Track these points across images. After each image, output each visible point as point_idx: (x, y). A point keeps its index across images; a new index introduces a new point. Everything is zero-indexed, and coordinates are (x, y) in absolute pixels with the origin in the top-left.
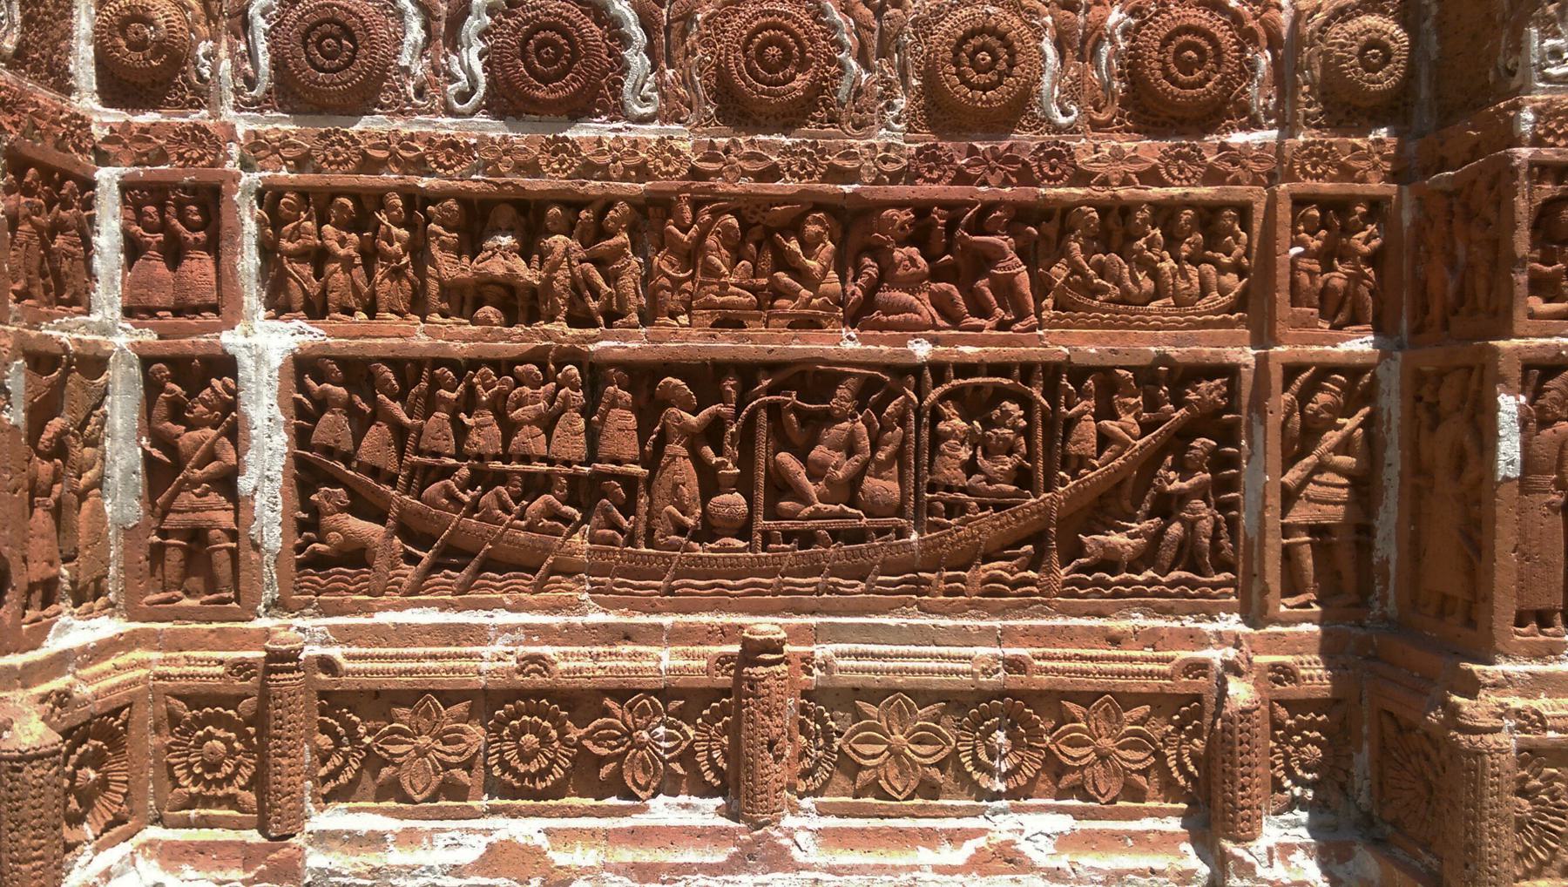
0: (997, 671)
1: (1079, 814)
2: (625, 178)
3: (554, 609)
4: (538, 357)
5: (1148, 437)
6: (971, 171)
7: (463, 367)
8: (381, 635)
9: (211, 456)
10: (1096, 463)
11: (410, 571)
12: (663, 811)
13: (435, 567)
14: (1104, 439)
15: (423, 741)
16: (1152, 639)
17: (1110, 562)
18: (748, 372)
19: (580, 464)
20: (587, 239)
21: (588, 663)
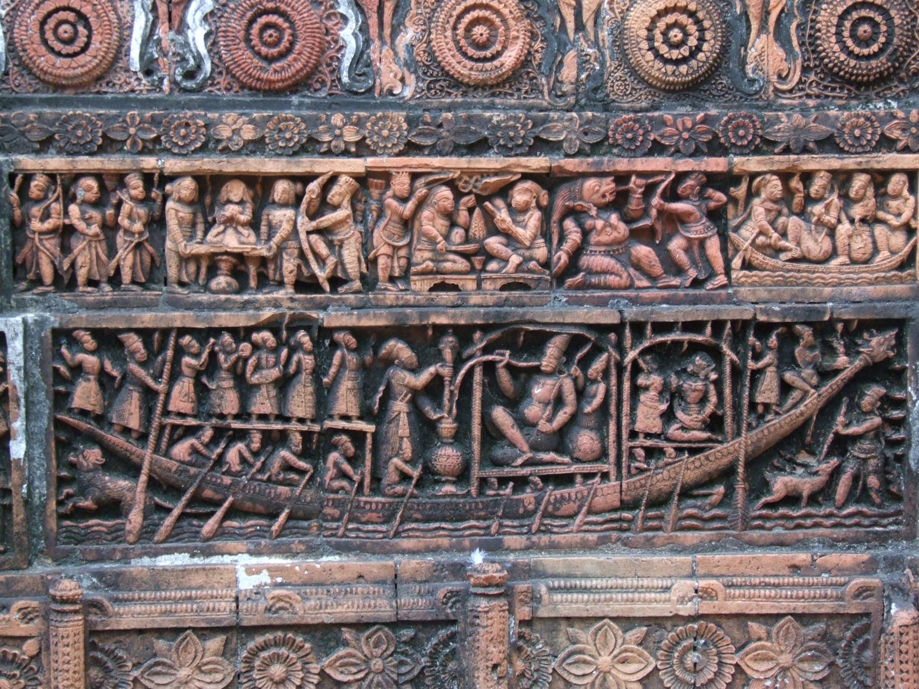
4: (273, 326)
7: (203, 335)
14: (785, 388)
17: (792, 499)
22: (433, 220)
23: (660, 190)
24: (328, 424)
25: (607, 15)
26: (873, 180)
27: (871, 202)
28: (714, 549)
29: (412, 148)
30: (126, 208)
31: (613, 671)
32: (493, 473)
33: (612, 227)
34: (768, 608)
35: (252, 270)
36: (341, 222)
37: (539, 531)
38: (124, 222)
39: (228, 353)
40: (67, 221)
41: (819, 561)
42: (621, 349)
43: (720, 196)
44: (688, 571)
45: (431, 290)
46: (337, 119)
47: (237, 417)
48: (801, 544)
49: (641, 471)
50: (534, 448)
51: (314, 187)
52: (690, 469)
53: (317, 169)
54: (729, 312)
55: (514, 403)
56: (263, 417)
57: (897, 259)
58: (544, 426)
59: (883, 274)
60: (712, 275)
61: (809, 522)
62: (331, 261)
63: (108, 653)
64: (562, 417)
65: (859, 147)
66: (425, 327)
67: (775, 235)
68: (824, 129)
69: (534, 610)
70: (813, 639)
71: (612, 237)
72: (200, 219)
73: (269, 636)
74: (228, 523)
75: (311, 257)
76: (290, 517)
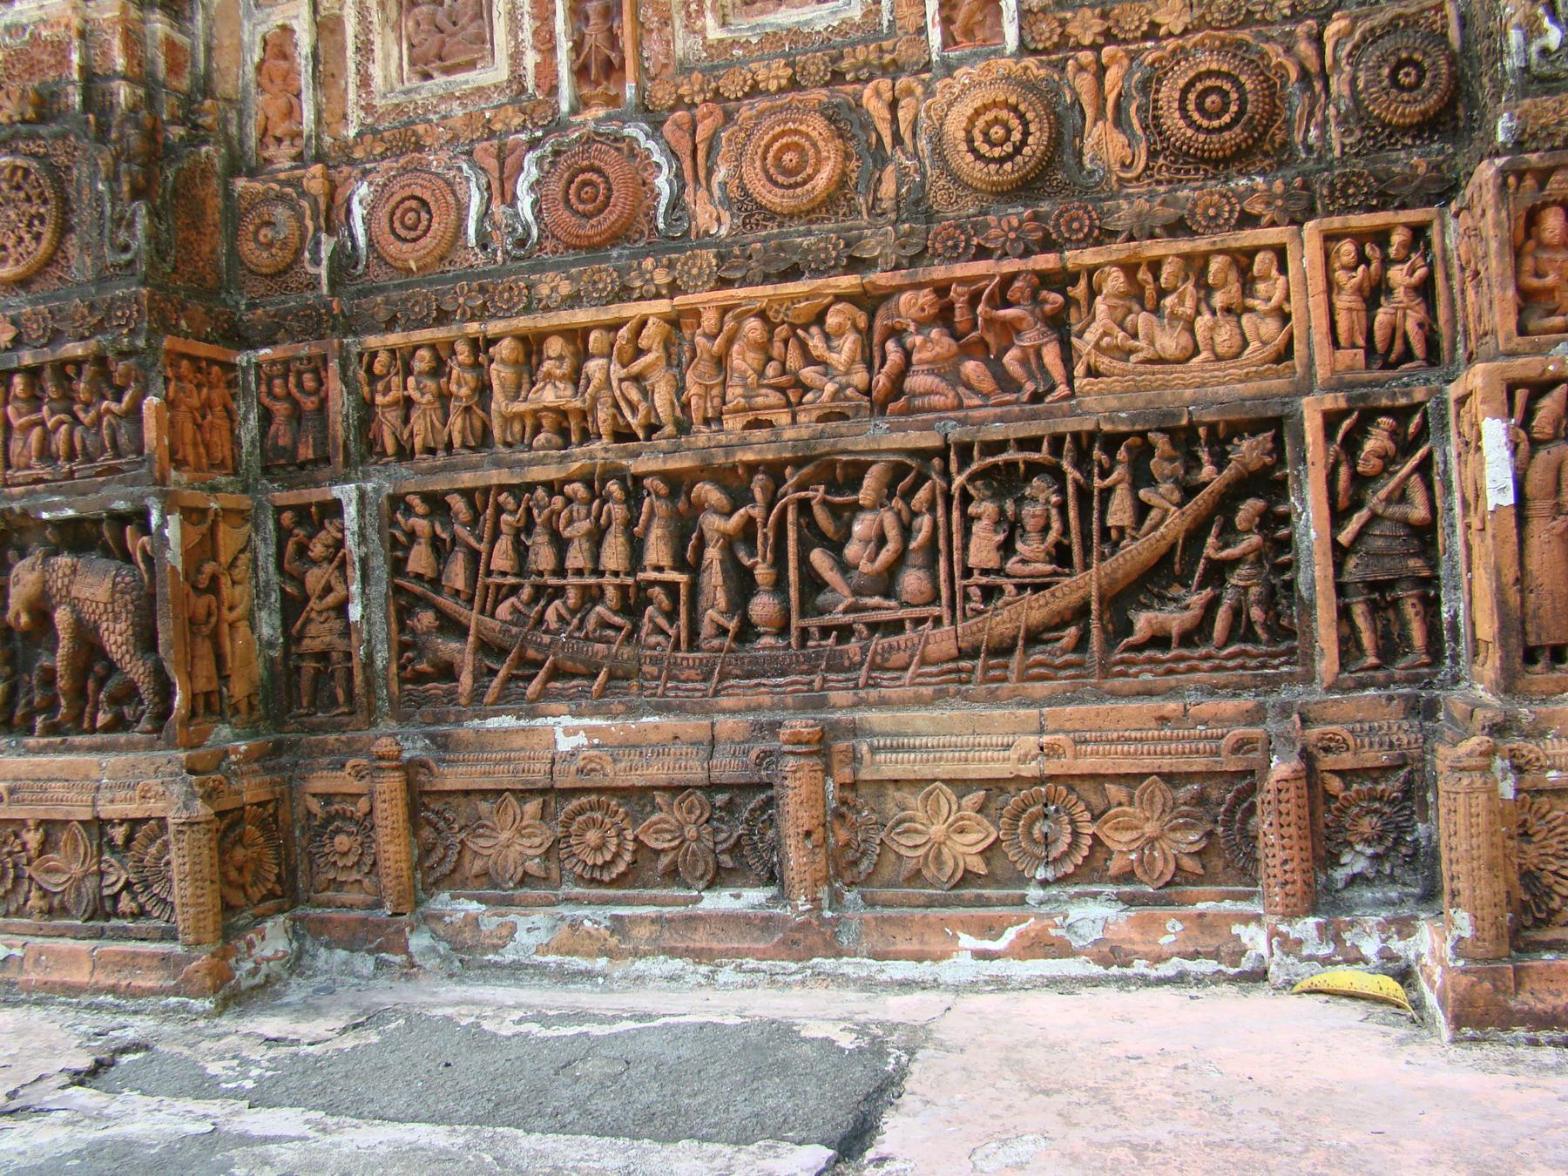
9: (328, 589)
14: (1142, 510)
17: (1159, 641)
20: (626, 358)
24: (641, 576)
25: (924, 123)
26: (1235, 262)
27: (1235, 287)
28: (1070, 701)
29: (724, 283)
32: (813, 623)
33: (936, 343)
34: (1127, 766)
35: (573, 424)
37: (867, 685)
38: (454, 388)
39: (541, 509)
41: (1192, 710)
42: (946, 475)
43: (1057, 298)
44: (1036, 726)
45: (745, 427)
46: (648, 263)
48: (1172, 692)
49: (979, 613)
50: (857, 592)
52: (1035, 609)
53: (625, 314)
54: (1067, 426)
56: (579, 572)
57: (1270, 350)
58: (865, 567)
60: (1053, 388)
61: (1182, 666)
62: (642, 408)
64: (885, 555)
65: (1214, 225)
66: (734, 467)
68: (1171, 213)
69: (855, 772)
72: (526, 377)
73: (584, 800)
74: (552, 684)
75: (623, 404)
76: (611, 676)
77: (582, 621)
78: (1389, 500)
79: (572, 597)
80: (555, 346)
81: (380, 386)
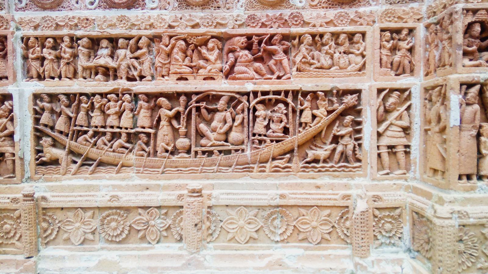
0: (276, 198)
1: (306, 249)
2: (146, 29)
3: (123, 179)
4: (115, 92)
5: (330, 116)
6: (267, 23)
8: (63, 189)
10: (311, 125)
11: (74, 167)
12: (161, 248)
13: (83, 165)
14: (314, 117)
15: (77, 225)
16: (332, 187)
17: (316, 161)
18: (188, 95)
19: (131, 129)
20: (133, 50)
21: (133, 198)
22: (177, 53)
23: (264, 41)
26: (349, 37)
27: (347, 44)
30: (63, 49)
31: (245, 227)
35: (111, 73)
36: (143, 54)
38: (63, 54)
40: (42, 55)
45: (177, 80)
47: (102, 127)
51: (132, 42)
55: (208, 122)
57: (358, 66)
59: (352, 73)
61: (323, 170)
63: (50, 216)
67: (309, 58)
70: (325, 216)
71: (246, 59)
73: (110, 211)
77: (112, 144)
78: (396, 119)
79: (108, 136)
80: (104, 43)
81: (31, 50)
